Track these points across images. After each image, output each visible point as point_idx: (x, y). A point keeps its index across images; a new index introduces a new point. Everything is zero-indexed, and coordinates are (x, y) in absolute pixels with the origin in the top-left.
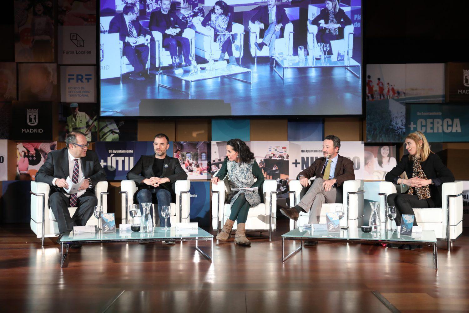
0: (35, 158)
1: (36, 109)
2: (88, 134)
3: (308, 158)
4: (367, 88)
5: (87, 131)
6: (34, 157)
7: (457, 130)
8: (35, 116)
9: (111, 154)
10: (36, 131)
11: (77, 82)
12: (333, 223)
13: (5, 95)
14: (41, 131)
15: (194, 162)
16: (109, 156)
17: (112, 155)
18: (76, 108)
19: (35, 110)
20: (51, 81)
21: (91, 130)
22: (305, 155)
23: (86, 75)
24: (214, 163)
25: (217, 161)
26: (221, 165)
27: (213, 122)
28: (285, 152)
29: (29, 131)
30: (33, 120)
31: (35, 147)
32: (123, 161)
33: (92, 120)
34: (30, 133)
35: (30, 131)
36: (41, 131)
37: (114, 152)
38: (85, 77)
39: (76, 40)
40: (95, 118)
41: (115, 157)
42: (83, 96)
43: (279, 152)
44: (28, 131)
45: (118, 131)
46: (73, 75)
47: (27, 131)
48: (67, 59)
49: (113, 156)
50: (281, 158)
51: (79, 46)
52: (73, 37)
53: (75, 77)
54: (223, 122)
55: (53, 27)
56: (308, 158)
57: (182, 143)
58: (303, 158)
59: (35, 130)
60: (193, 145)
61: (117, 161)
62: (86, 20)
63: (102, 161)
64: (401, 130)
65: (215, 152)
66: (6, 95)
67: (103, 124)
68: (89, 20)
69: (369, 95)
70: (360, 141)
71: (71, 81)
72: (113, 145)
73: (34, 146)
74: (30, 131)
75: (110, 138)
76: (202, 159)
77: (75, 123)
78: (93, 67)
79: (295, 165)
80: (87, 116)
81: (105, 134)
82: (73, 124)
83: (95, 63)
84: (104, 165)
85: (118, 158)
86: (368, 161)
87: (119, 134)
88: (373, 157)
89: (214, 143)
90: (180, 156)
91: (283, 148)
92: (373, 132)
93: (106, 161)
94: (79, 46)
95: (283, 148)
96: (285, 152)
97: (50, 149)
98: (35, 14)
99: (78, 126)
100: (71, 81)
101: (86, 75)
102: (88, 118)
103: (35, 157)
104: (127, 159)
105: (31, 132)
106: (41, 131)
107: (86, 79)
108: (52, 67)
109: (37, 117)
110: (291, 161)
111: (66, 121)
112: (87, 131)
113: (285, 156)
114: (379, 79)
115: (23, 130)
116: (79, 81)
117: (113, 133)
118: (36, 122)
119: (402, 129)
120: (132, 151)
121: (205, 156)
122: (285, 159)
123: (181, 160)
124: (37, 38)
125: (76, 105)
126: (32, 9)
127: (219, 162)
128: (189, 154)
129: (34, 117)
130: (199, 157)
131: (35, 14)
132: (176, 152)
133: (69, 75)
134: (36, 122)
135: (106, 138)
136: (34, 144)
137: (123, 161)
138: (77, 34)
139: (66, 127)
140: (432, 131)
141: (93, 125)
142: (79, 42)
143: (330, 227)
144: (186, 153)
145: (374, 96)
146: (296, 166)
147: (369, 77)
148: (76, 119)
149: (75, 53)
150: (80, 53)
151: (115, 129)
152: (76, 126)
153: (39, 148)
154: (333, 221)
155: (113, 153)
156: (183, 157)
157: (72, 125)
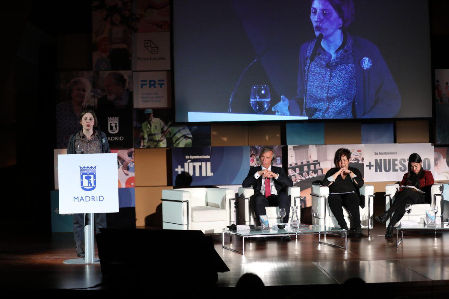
1: (117, 117)
2: (163, 140)
3: (381, 160)
4: (436, 92)
5: (162, 137)
8: (116, 124)
10: (117, 139)
11: (150, 87)
12: (431, 219)
13: (83, 104)
14: (121, 138)
16: (186, 162)
17: (189, 161)
18: (150, 114)
19: (116, 118)
20: (126, 88)
21: (166, 136)
22: (379, 157)
23: (159, 81)
24: (291, 167)
25: (294, 165)
26: (297, 169)
28: (360, 155)
29: (110, 139)
30: (114, 128)
32: (200, 167)
33: (167, 125)
34: (111, 141)
37: (191, 158)
38: (157, 82)
39: (150, 46)
40: (169, 123)
41: (192, 163)
43: (354, 155)
45: (191, 136)
46: (146, 81)
47: (108, 139)
49: (191, 162)
50: (356, 161)
51: (153, 52)
53: (148, 83)
56: (381, 160)
57: (256, 147)
58: (376, 161)
59: (116, 138)
61: (194, 167)
63: (179, 167)
65: (292, 156)
66: (84, 103)
67: (176, 129)
68: (163, 27)
69: (439, 98)
70: (430, 142)
71: (144, 86)
72: (187, 151)
75: (182, 144)
76: (277, 163)
77: (150, 129)
78: (165, 72)
80: (161, 121)
81: (178, 139)
82: (148, 130)
83: (169, 68)
84: (181, 171)
85: (195, 164)
86: (437, 162)
87: (192, 139)
88: (442, 158)
89: (290, 147)
90: (254, 160)
91: (358, 151)
93: (183, 167)
95: (358, 151)
96: (360, 155)
97: (127, 156)
99: (153, 132)
100: (144, 86)
102: (163, 123)
104: (204, 164)
105: (112, 140)
106: (122, 138)
107: (159, 84)
109: (118, 125)
110: (366, 163)
111: (141, 127)
112: (162, 137)
113: (360, 159)
117: (186, 138)
118: (116, 129)
120: (208, 157)
121: (280, 160)
122: (360, 162)
123: (256, 164)
124: (114, 46)
125: (150, 111)
127: (296, 166)
129: (115, 125)
132: (251, 156)
133: (142, 81)
134: (116, 129)
135: (179, 143)
137: (200, 167)
138: (151, 41)
139: (141, 134)
141: (167, 131)
143: (429, 221)
145: (443, 100)
146: (370, 169)
147: (438, 81)
148: (151, 125)
150: (154, 59)
151: (188, 134)
152: (151, 132)
154: (431, 217)
155: (190, 159)
156: (258, 162)
157: (147, 132)
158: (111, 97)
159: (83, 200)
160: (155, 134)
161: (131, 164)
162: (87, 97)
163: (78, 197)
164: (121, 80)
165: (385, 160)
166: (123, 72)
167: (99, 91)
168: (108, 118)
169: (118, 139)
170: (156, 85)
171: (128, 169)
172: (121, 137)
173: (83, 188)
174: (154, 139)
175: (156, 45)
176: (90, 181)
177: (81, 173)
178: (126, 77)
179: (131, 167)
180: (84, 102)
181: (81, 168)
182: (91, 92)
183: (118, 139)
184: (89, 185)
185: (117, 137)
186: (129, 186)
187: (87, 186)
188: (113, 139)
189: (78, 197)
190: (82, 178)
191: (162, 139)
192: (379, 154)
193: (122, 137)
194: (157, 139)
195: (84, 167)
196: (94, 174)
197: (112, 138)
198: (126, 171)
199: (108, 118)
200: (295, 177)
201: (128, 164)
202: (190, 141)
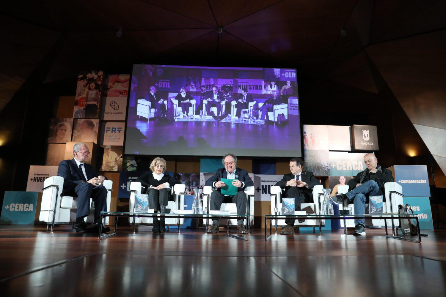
7: (361, 169)
9: (130, 179)
11: (112, 132)
15: (188, 187)
16: (129, 181)
17: (131, 181)
18: (109, 148)
21: (118, 163)
23: (118, 128)
27: (202, 160)
38: (117, 129)
39: (114, 105)
42: (115, 141)
45: (136, 165)
46: (110, 128)
48: (106, 117)
51: (115, 109)
52: (112, 104)
53: (111, 129)
54: (208, 160)
55: (100, 96)
56: (266, 186)
57: (180, 174)
60: (187, 176)
64: (327, 168)
68: (124, 94)
75: (130, 169)
76: (193, 185)
77: (108, 159)
79: (257, 191)
80: (116, 153)
89: (201, 174)
92: (309, 169)
94: (115, 109)
98: (90, 89)
100: (108, 131)
101: (118, 128)
102: (116, 155)
107: (118, 130)
108: (96, 122)
112: (115, 164)
114: (311, 134)
116: (113, 132)
119: (327, 167)
124: (89, 103)
126: (88, 86)
128: (184, 182)
130: (191, 184)
131: (90, 89)
133: (107, 128)
140: (345, 169)
142: (116, 107)
144: (182, 181)
147: (305, 133)
148: (108, 156)
149: (112, 114)
151: (134, 164)
155: (131, 179)
160: (111, 162)
166: (93, 120)
170: (116, 131)
191: (115, 165)
192: (265, 182)
194: (112, 165)
202: (135, 168)
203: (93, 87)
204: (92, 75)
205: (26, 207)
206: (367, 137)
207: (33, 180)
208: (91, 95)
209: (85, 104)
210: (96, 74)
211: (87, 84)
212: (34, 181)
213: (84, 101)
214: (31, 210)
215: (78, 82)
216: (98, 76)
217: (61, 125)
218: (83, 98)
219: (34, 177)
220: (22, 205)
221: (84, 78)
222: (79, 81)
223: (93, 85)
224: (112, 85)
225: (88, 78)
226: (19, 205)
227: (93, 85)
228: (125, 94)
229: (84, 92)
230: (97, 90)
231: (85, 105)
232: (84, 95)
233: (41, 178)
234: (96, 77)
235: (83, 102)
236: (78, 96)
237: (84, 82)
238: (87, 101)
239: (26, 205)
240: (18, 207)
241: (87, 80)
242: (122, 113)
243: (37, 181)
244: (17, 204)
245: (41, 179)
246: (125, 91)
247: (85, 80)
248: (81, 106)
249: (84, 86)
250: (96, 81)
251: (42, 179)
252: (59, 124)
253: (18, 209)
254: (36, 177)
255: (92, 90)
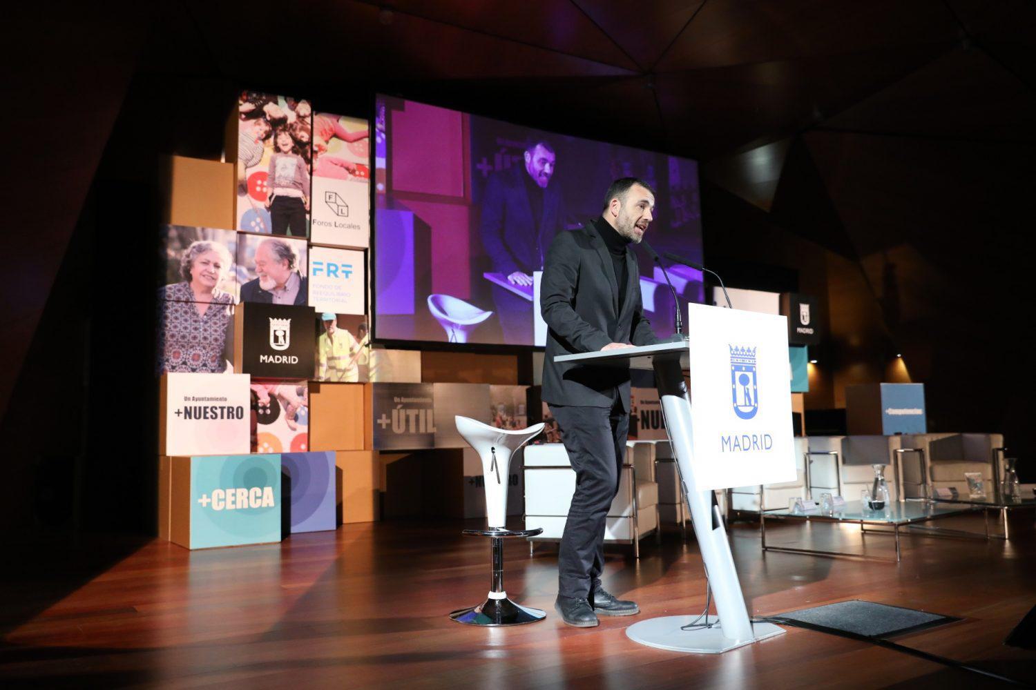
0: (268, 412)
1: (287, 319)
6: (267, 408)
8: (285, 332)
9: (398, 404)
11: (328, 275)
13: (213, 292)
15: (509, 418)
16: (395, 408)
17: (399, 406)
20: (295, 270)
21: (357, 361)
23: (343, 266)
29: (272, 360)
30: (281, 339)
31: (268, 390)
32: (417, 417)
34: (275, 364)
35: (274, 360)
36: (295, 360)
44: (271, 359)
46: (321, 264)
51: (340, 214)
53: (325, 267)
59: (284, 359)
62: (352, 172)
68: (357, 173)
71: (317, 272)
73: (267, 389)
74: (274, 360)
77: (331, 349)
82: (328, 349)
93: (390, 416)
98: (277, 149)
99: (336, 355)
100: (317, 272)
101: (343, 266)
103: (270, 408)
105: (277, 362)
106: (295, 360)
107: (343, 272)
115: (262, 357)
124: (280, 192)
126: (272, 139)
129: (283, 334)
136: (267, 386)
137: (417, 417)
142: (340, 208)
148: (332, 341)
149: (333, 224)
153: (276, 393)
156: (494, 411)
158: (267, 285)
159: (739, 445)
161: (302, 409)
162: (222, 280)
163: (729, 438)
164: (287, 256)
165: (652, 412)
167: (244, 270)
168: (271, 319)
169: (288, 360)
170: (339, 272)
171: (296, 418)
172: (293, 357)
173: (736, 410)
174: (338, 367)
175: (329, 206)
176: (748, 389)
177: (732, 366)
178: (295, 250)
179: (301, 415)
180: (216, 288)
181: (731, 349)
182: (230, 270)
183: (288, 360)
184: (748, 404)
185: (286, 357)
186: (297, 451)
187: (744, 404)
188: (278, 359)
189: (729, 438)
190: (734, 382)
193: (295, 357)
195: (737, 350)
196: (754, 369)
197: (276, 359)
198: (292, 423)
199: (271, 319)
200: (553, 436)
201: (296, 409)
203: (286, 145)
204: (278, 109)
205: (256, 498)
206: (805, 318)
207: (182, 416)
208: (284, 168)
209: (269, 195)
210: (293, 108)
211: (267, 136)
212: (185, 418)
213: (265, 183)
214: (268, 504)
215: (241, 122)
216: (299, 116)
217: (200, 250)
218: (261, 175)
219: (186, 408)
220: (245, 491)
221: (257, 114)
222: (244, 120)
223: (285, 140)
224: (323, 143)
225: (270, 116)
226: (236, 491)
227: (285, 140)
228: (360, 176)
229: (262, 156)
230: (300, 156)
231: (270, 198)
232: (264, 167)
233: (205, 408)
234: (292, 118)
235: (262, 186)
236: (246, 168)
237: (257, 128)
238: (274, 185)
239: (253, 490)
240: (233, 499)
241: (267, 122)
242: (359, 227)
243: (195, 417)
244: (230, 491)
245: (206, 413)
246: (360, 166)
247: (261, 120)
248: (260, 196)
249: (259, 139)
250: (294, 130)
251: (208, 410)
252: (195, 244)
253: (234, 503)
254: (191, 408)
255: (286, 153)
